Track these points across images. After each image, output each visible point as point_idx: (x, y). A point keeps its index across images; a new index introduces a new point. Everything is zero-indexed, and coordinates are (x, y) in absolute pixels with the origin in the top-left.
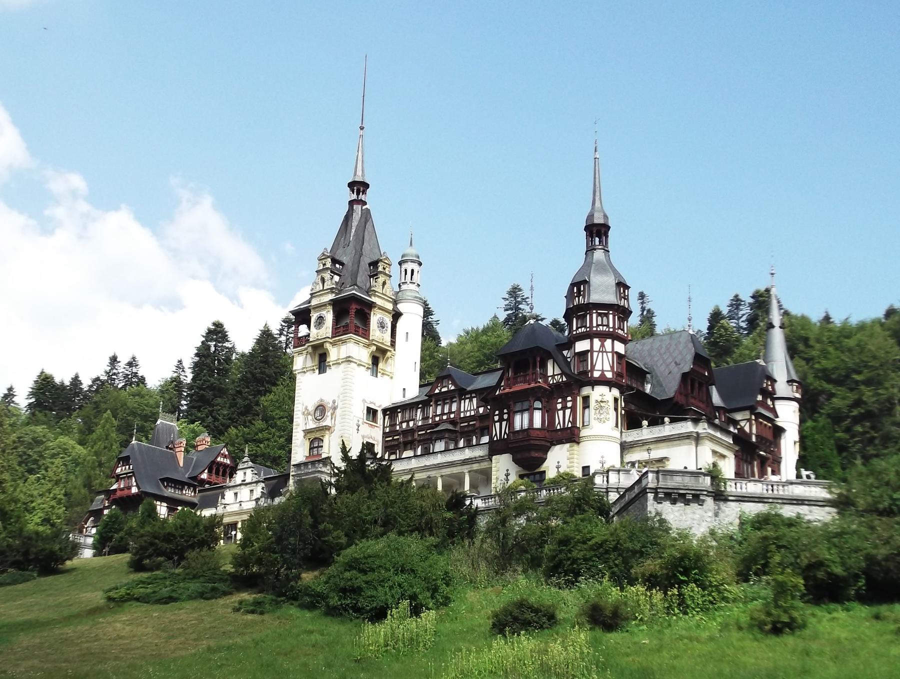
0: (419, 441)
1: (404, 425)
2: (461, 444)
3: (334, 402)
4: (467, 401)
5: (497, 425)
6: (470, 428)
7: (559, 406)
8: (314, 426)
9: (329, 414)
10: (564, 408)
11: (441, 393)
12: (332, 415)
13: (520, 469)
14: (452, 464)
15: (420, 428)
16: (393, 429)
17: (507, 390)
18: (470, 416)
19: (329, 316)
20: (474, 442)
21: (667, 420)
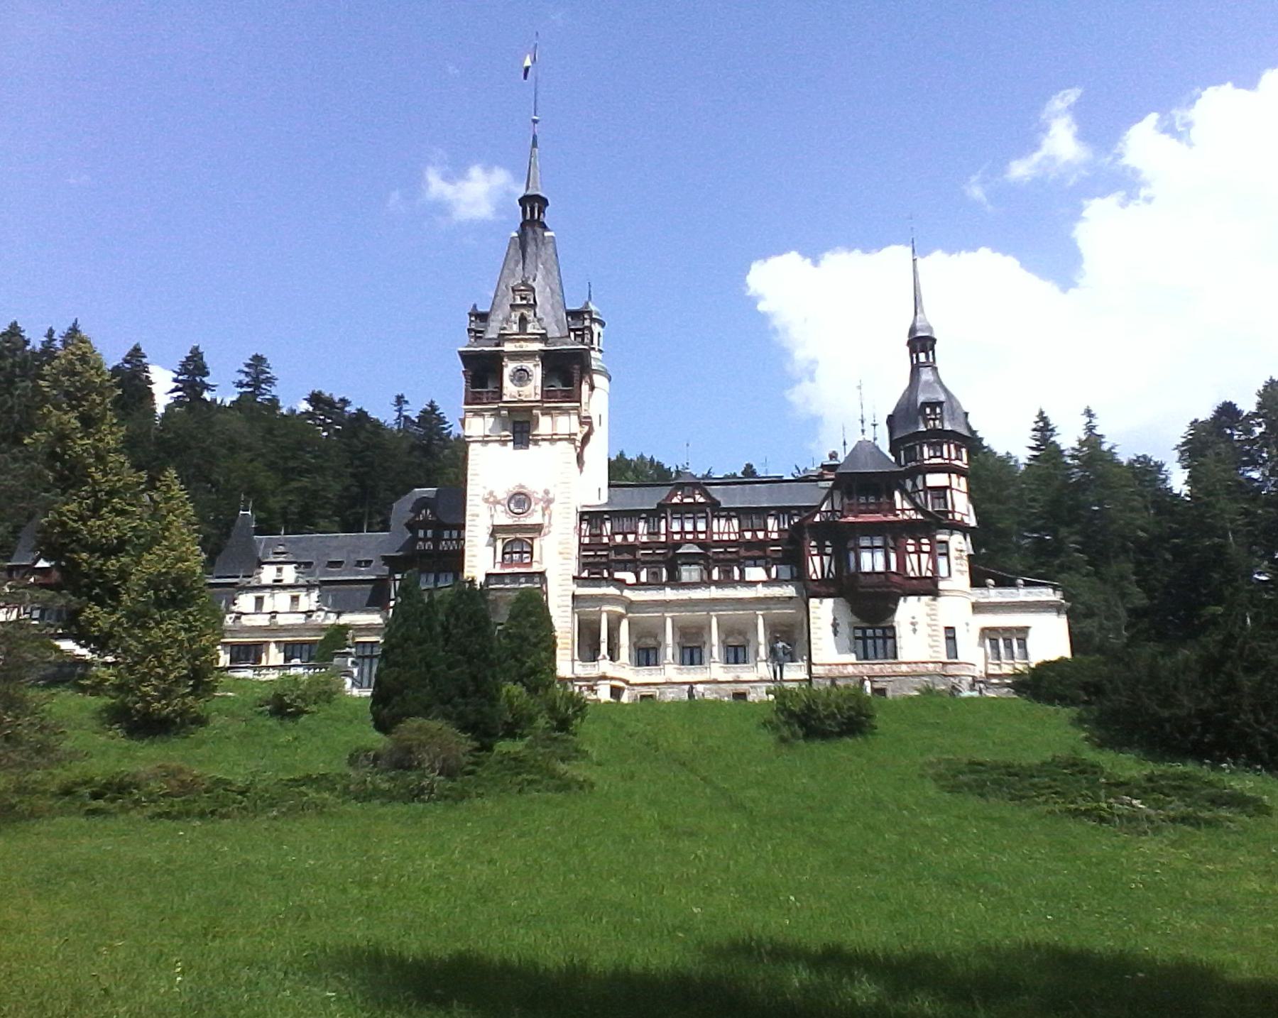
0: (645, 563)
1: (619, 538)
2: (715, 574)
3: (547, 492)
4: (723, 521)
5: (817, 559)
6: (729, 556)
7: (911, 549)
8: (509, 521)
9: (539, 508)
10: (919, 552)
11: (682, 504)
12: (544, 510)
13: (855, 619)
14: (740, 601)
15: (645, 546)
16: (596, 540)
17: (851, 519)
18: (730, 541)
19: (537, 372)
20: (737, 577)
21: (1020, 581)
